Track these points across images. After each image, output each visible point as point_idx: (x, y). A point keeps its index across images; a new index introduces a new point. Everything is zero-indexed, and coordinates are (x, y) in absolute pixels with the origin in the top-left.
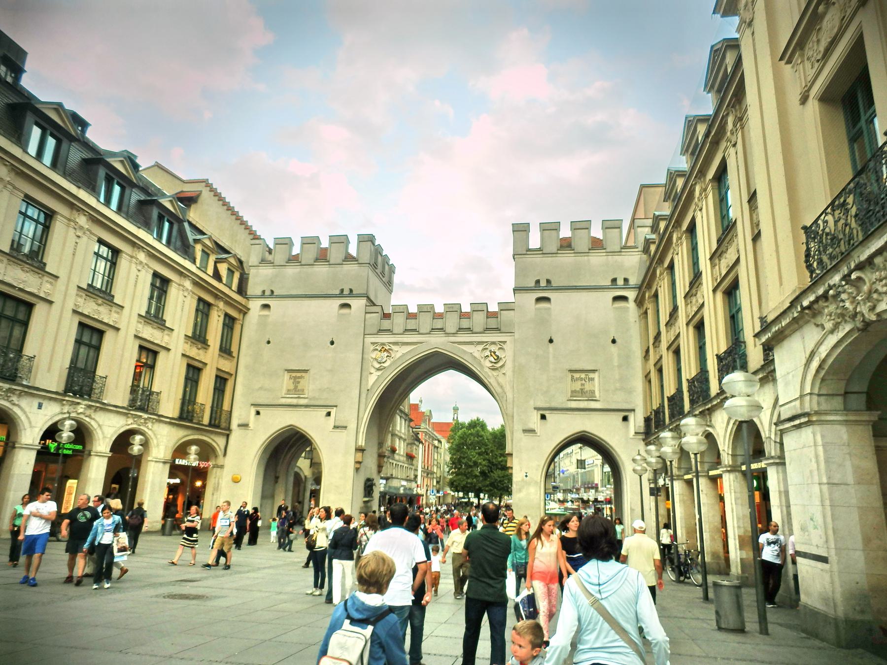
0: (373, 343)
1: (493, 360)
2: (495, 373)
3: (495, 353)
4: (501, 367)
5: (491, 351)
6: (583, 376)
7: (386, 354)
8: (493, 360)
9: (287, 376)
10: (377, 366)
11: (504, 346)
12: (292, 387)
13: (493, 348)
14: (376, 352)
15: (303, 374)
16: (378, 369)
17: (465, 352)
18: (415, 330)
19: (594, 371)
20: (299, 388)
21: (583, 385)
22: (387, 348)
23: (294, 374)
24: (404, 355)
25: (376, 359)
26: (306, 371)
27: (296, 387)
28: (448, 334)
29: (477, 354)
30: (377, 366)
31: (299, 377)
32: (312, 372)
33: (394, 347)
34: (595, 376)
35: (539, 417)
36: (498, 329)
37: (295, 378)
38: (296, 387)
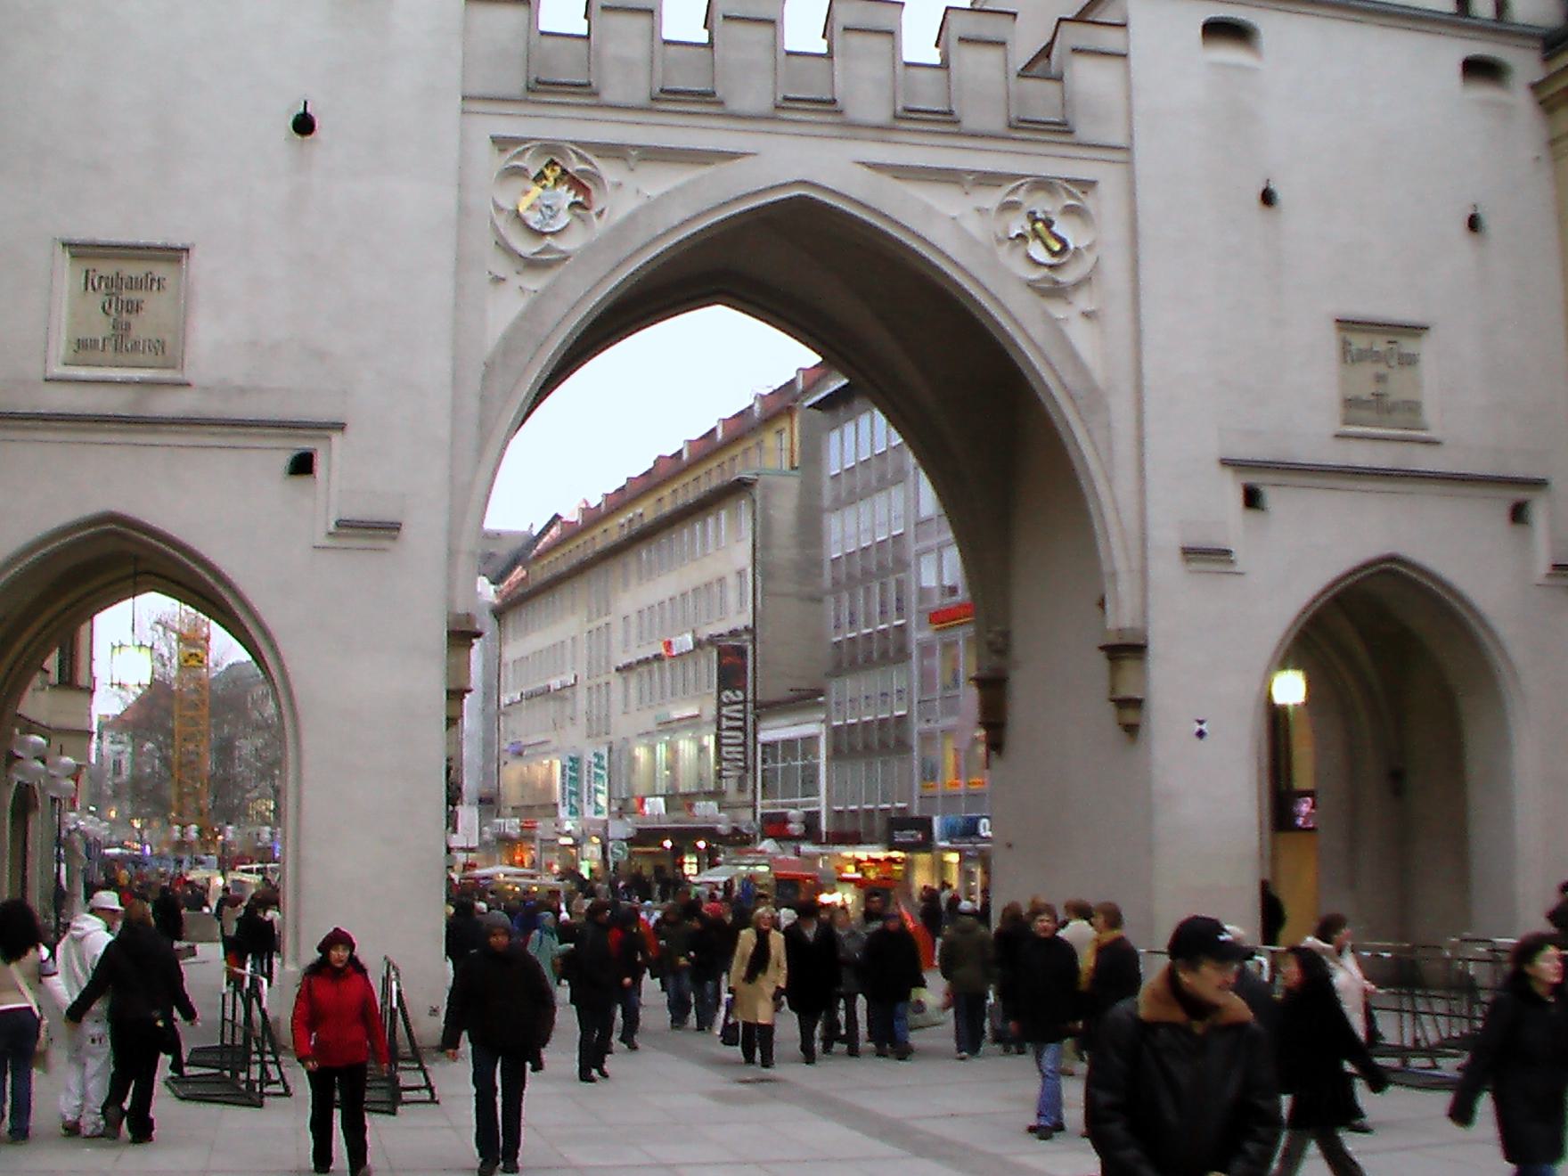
0: (502, 143)
1: (1040, 254)
2: (1058, 310)
3: (1049, 224)
4: (1077, 285)
5: (1033, 218)
6: (1380, 344)
7: (566, 196)
8: (1040, 254)
9: (68, 275)
10: (527, 247)
11: (1089, 202)
12: (100, 328)
13: (1042, 204)
14: (519, 183)
15: (160, 270)
16: (532, 264)
17: (928, 211)
18: (706, 96)
19: (1416, 330)
20: (141, 328)
21: (1380, 378)
22: (575, 166)
23: (107, 269)
24: (653, 206)
25: (517, 214)
26: (175, 254)
27: (121, 332)
28: (854, 128)
29: (973, 225)
30: (527, 247)
31: (135, 284)
32: (200, 265)
33: (609, 171)
34: (1425, 348)
35: (1236, 497)
36: (1062, 129)
37: (114, 283)
38: (121, 332)
